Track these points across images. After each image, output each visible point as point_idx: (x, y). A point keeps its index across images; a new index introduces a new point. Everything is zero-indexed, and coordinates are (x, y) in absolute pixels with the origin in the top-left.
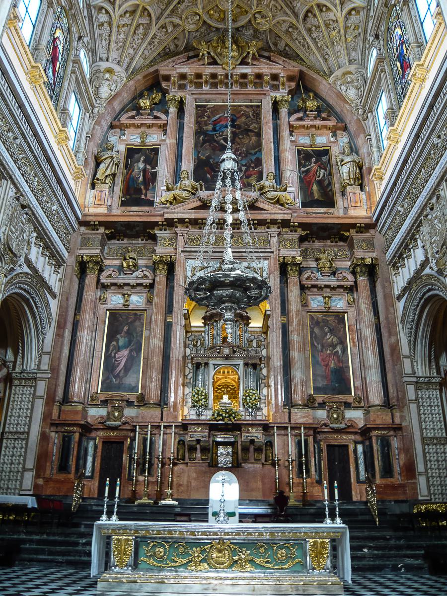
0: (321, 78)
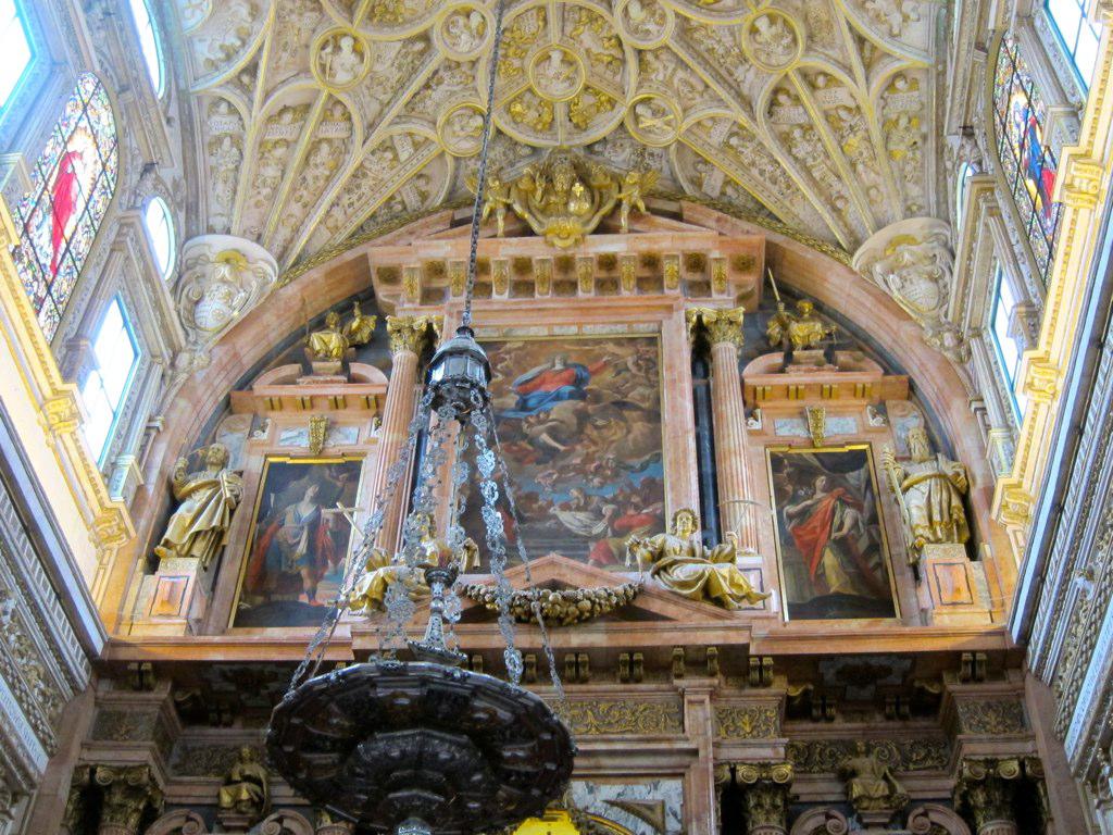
0: (827, 259)
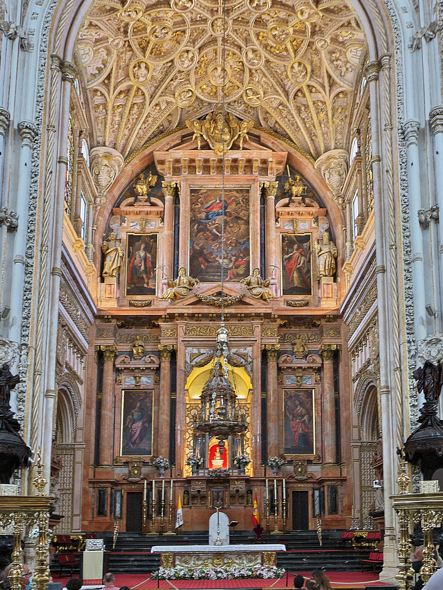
0: (307, 161)
